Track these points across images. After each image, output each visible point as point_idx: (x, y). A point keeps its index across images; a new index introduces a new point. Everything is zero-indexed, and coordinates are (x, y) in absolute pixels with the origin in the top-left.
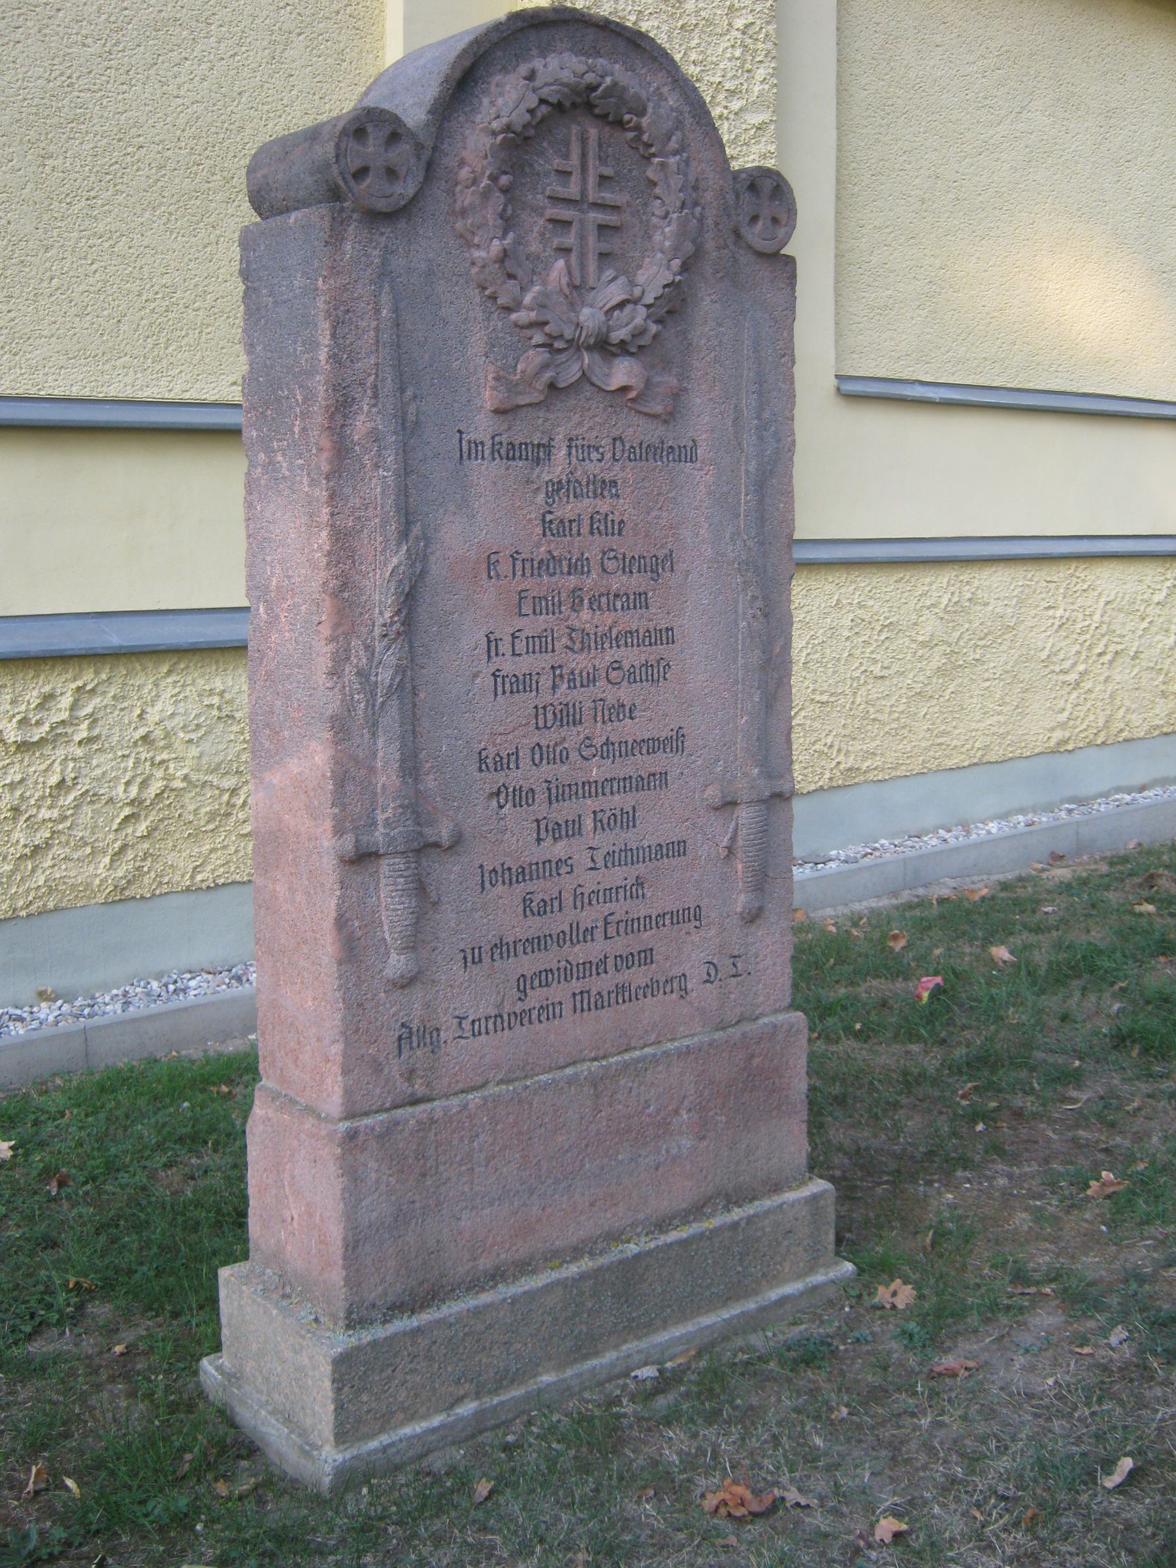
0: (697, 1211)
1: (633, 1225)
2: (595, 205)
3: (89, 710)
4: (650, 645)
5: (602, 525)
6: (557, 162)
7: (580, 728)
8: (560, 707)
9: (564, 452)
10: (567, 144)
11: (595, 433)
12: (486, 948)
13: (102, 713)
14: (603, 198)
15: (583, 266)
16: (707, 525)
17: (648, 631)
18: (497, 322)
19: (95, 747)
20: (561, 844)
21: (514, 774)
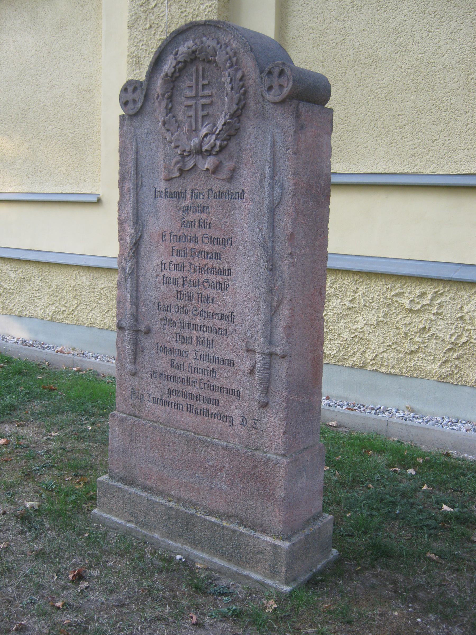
3: (438, 302)
6: (188, 83)
7: (193, 303)
9: (190, 194)
11: (201, 188)
12: (158, 373)
13: (444, 304)
17: (220, 269)
19: (440, 317)
20: (185, 345)
21: (169, 314)
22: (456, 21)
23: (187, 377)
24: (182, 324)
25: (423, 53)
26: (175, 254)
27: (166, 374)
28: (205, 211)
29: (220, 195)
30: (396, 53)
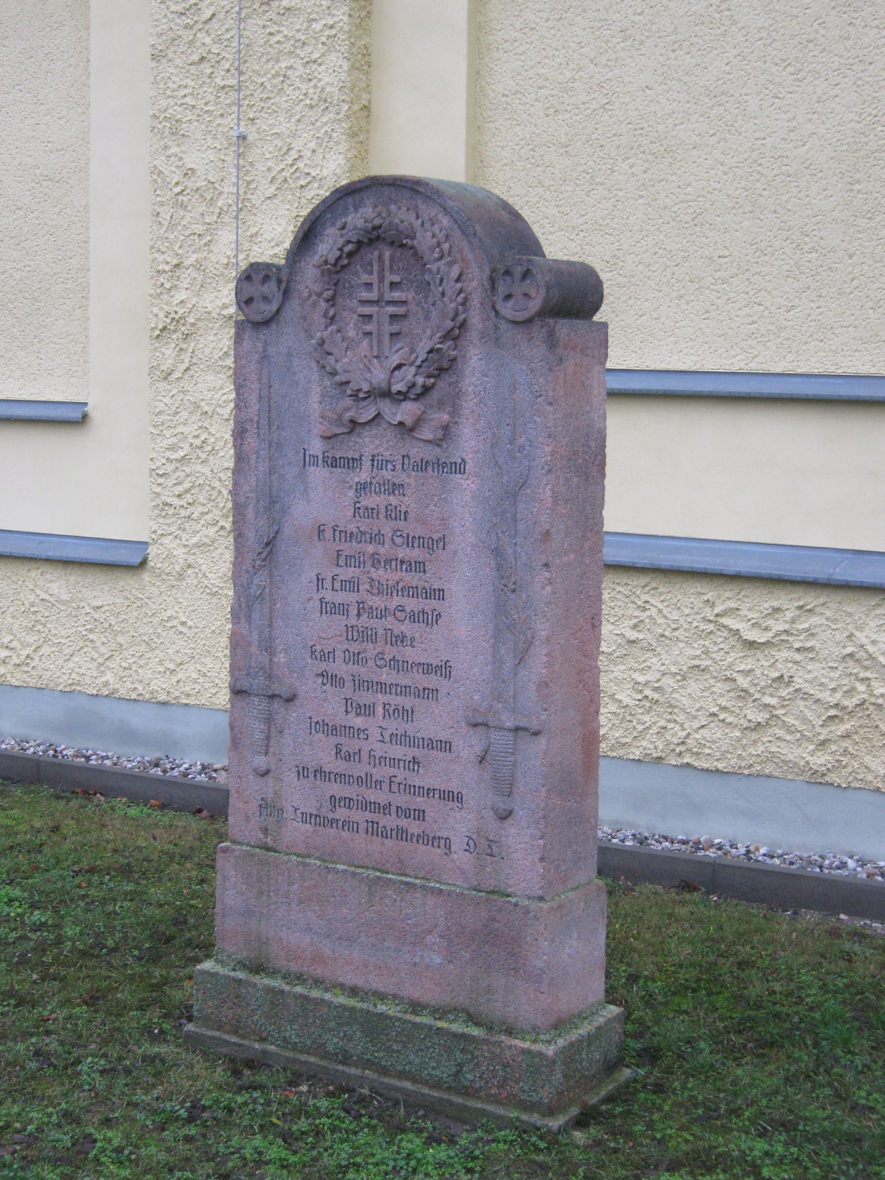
0: (440, 1012)
1: (395, 996)
2: (389, 303)
3: (806, 625)
4: (426, 598)
5: (393, 513)
6: (365, 278)
8: (361, 629)
10: (371, 265)
12: (311, 770)
14: (393, 297)
15: (380, 342)
16: (471, 520)
17: (424, 588)
18: (327, 382)
19: (810, 656)
21: (332, 665)
22: (827, 79)
23: (367, 774)
24: (357, 682)
25: (764, 139)
26: (342, 562)
27: (327, 770)
28: (396, 492)
29: (422, 466)
30: (712, 136)
